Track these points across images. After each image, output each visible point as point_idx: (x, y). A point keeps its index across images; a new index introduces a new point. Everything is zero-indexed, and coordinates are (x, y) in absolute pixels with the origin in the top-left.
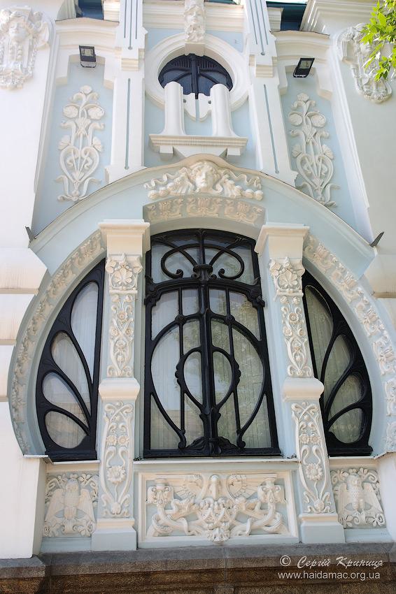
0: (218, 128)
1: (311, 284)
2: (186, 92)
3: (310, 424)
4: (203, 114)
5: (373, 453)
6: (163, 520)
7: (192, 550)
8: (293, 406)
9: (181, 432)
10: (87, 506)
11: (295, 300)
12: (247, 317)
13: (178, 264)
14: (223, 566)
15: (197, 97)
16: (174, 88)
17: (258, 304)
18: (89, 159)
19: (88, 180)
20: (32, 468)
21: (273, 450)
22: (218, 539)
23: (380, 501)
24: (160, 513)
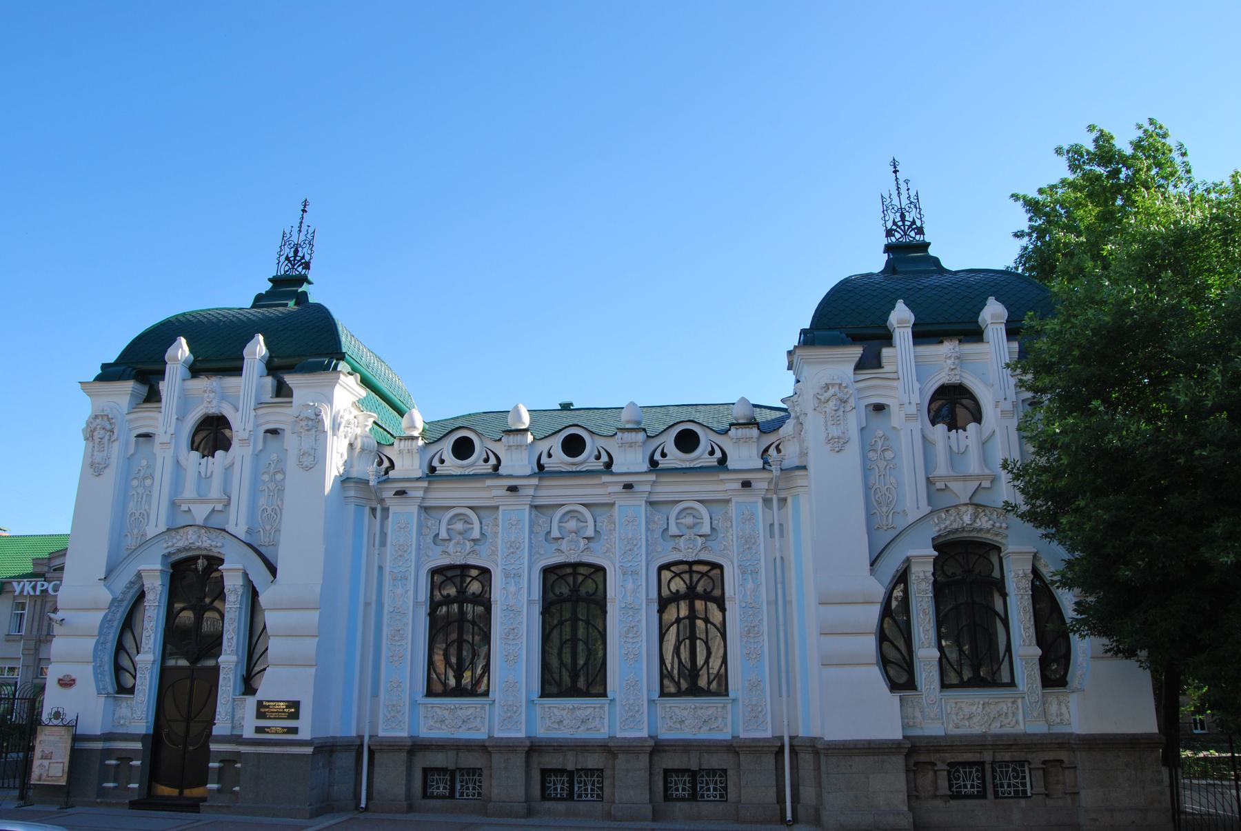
0: (973, 465)
2: (950, 430)
3: (1033, 673)
5: (1067, 687)
6: (956, 721)
7: (972, 736)
8: (1024, 663)
10: (918, 714)
11: (1026, 597)
14: (987, 743)
15: (957, 432)
16: (941, 428)
18: (890, 496)
19: (891, 513)
20: (895, 699)
21: (1012, 684)
22: (984, 731)
23: (1069, 712)
24: (954, 717)
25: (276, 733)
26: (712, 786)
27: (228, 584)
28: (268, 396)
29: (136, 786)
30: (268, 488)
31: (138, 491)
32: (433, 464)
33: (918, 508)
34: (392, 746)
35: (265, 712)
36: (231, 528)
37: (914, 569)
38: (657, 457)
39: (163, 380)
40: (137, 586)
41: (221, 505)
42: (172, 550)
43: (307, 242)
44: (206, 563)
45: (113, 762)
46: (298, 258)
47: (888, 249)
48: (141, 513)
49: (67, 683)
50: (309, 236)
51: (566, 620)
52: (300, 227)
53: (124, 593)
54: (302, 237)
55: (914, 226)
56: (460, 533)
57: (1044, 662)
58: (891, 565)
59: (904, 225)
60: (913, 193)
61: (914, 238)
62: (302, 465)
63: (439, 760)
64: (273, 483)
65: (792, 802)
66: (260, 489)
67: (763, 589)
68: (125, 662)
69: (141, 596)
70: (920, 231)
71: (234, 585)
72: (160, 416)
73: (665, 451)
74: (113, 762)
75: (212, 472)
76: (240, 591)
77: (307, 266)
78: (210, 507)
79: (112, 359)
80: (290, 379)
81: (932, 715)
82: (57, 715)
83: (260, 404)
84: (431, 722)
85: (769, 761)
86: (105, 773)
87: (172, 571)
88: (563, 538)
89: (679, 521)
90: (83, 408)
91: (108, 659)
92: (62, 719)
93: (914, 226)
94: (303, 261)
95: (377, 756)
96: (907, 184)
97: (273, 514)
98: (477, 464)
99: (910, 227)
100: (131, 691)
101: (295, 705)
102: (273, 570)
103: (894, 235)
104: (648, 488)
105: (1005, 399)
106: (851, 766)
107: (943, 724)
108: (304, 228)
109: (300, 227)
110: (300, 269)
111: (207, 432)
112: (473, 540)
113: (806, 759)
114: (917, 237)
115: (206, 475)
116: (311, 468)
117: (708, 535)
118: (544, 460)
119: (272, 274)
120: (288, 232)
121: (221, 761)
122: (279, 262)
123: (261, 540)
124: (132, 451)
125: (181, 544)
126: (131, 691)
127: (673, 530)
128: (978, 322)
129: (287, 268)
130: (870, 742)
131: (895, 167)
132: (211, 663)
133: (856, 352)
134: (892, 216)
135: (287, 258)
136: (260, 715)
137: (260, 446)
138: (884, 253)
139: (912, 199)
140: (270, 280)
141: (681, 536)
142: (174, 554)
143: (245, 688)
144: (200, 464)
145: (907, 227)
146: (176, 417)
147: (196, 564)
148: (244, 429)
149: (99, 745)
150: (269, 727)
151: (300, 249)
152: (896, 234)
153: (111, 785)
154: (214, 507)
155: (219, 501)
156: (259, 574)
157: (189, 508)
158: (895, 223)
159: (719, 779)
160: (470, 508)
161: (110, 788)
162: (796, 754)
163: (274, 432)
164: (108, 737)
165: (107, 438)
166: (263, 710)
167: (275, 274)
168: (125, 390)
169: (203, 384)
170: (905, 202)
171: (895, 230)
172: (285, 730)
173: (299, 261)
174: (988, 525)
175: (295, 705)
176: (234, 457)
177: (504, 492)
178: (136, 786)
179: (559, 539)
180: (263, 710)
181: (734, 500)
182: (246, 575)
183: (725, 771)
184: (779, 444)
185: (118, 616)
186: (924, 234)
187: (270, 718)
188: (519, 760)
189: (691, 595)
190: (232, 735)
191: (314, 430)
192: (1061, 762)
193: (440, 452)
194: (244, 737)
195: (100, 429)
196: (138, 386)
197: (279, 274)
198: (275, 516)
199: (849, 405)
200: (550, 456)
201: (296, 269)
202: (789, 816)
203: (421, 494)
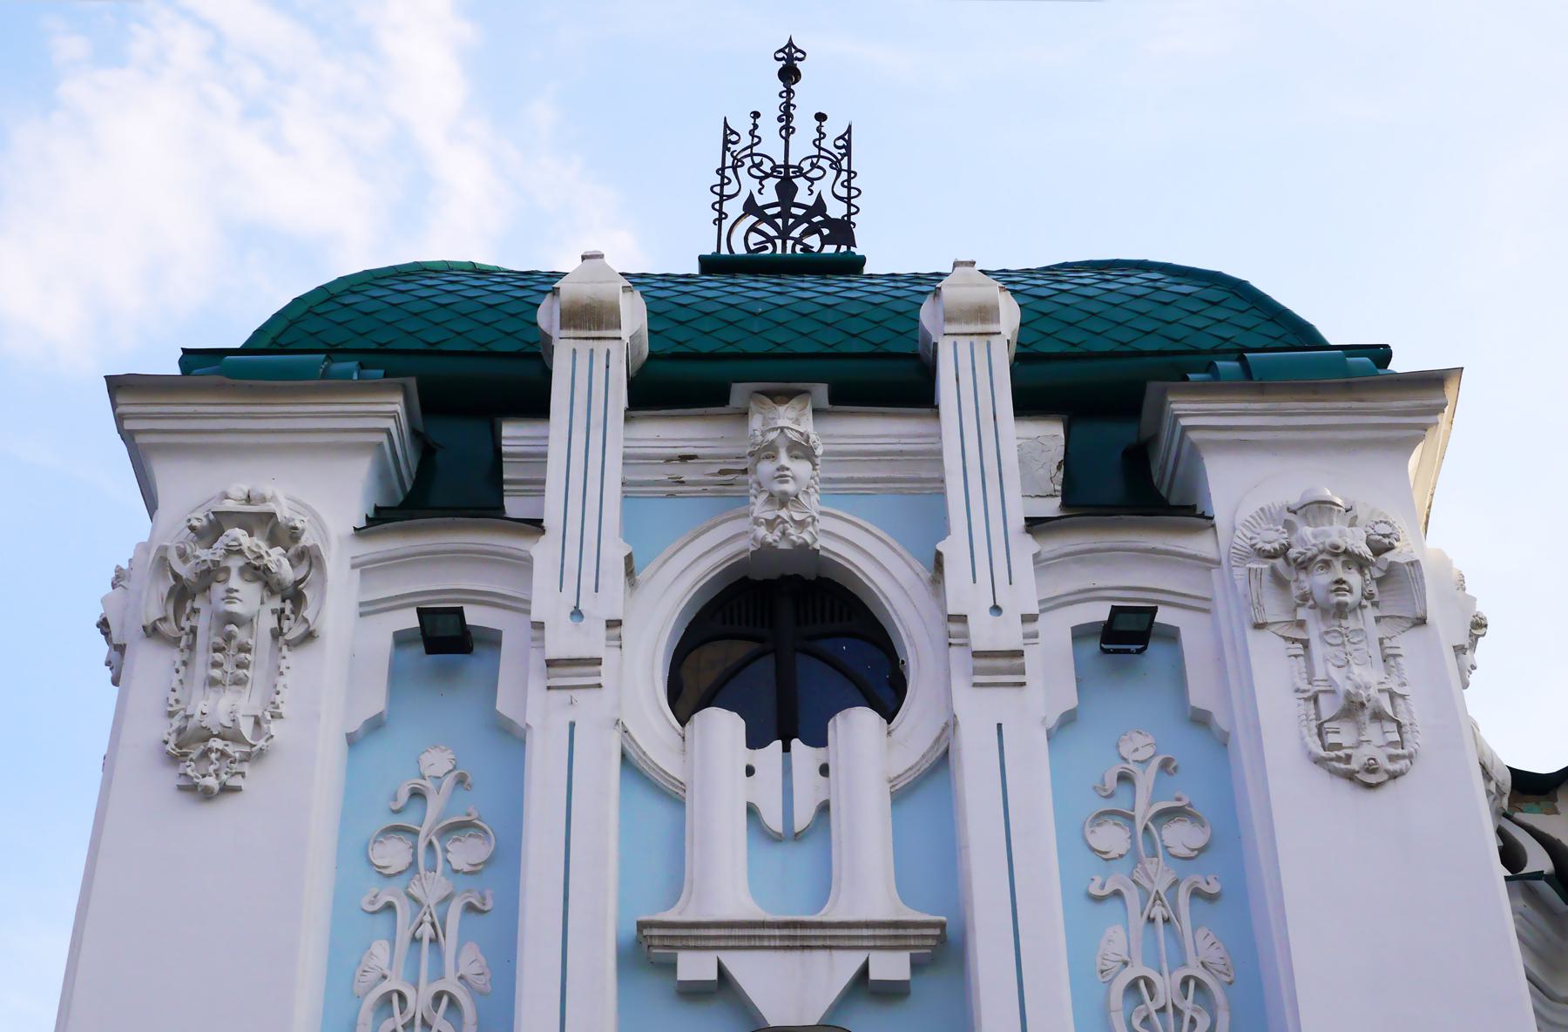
31: (415, 890)
43: (824, 163)
48: (438, 997)
50: (827, 144)
52: (786, 115)
54: (801, 148)
62: (1348, 758)
66: (1095, 890)
72: (542, 552)
75: (824, 808)
77: (842, 231)
78: (846, 965)
97: (1188, 1006)
108: (803, 121)
109: (786, 115)
111: (741, 649)
116: (1394, 776)
120: (742, 125)
122: (722, 216)
124: (376, 702)
129: (755, 238)
135: (750, 207)
144: (750, 771)
148: (996, 609)
151: (800, 182)
154: (864, 970)
155: (891, 934)
157: (721, 970)
165: (268, 622)
191: (1370, 613)
195: (242, 571)
197: (725, 251)
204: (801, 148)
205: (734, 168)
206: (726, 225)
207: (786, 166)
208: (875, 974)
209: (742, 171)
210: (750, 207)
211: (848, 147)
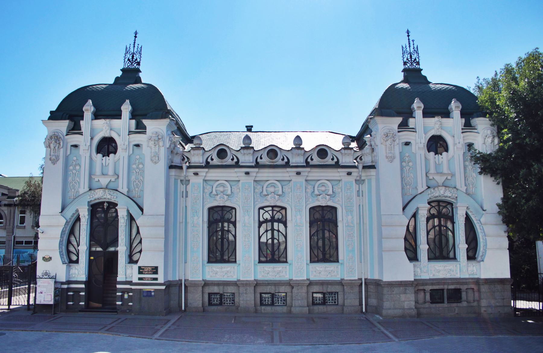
1: (468, 220)
2: (435, 155)
4: (440, 162)
9: (435, 254)
12: (449, 225)
13: (433, 211)
16: (432, 154)
17: (453, 223)
25: (148, 280)
26: (331, 299)
27: (120, 214)
28: (133, 129)
29: (83, 303)
30: (136, 171)
32: (208, 160)
33: (422, 187)
34: (195, 284)
35: (142, 271)
36: (120, 189)
37: (420, 212)
38: (309, 160)
39: (83, 119)
40: (75, 215)
41: (114, 179)
42: (92, 199)
43: (138, 52)
44: (107, 205)
45: (72, 293)
46: (134, 60)
47: (404, 71)
49: (47, 259)
50: (139, 49)
51: (269, 230)
52: (134, 45)
53: (70, 219)
54: (136, 50)
55: (415, 61)
56: (222, 192)
57: (468, 250)
58: (411, 210)
59: (411, 60)
60: (415, 47)
61: (415, 66)
63: (216, 289)
64: (138, 169)
65: (365, 305)
67: (355, 218)
68: (72, 249)
69: (78, 219)
70: (418, 63)
71: (123, 215)
73: (313, 157)
74: (72, 293)
75: (109, 163)
76: (126, 218)
77: (139, 64)
79: (54, 109)
80: (146, 122)
81: (425, 271)
82: (46, 274)
83: (130, 133)
84: (211, 274)
85: (357, 289)
86: (68, 298)
87: (91, 208)
88: (268, 195)
89: (318, 188)
90: (44, 132)
91: (64, 248)
92: (49, 276)
93: (415, 61)
94: (136, 61)
95: (189, 288)
96: (413, 42)
98: (228, 161)
99: (414, 61)
100: (77, 262)
101: (156, 268)
102: (142, 210)
103: (407, 65)
104: (306, 174)
105: (459, 143)
106: (393, 291)
107: (429, 274)
109: (134, 45)
110: (135, 65)
112: (228, 195)
113: (372, 288)
114: (417, 66)
115: (105, 165)
117: (331, 195)
118: (259, 160)
119: (122, 67)
120: (128, 47)
121: (122, 292)
122: (125, 61)
123: (134, 194)
125: (97, 197)
126: (77, 262)
127: (316, 192)
128: (448, 109)
129: (129, 65)
130: (401, 282)
131: (408, 34)
132: (112, 249)
133: (399, 120)
134: (406, 56)
135: (129, 60)
136: (140, 273)
137: (131, 152)
138: (402, 72)
139: (415, 49)
140: (121, 70)
141: (320, 195)
142: (93, 201)
143: (130, 260)
145: (412, 61)
146: (90, 138)
147: (103, 205)
149: (65, 286)
150: (144, 278)
151: (135, 55)
152: (408, 64)
153: (71, 303)
154: (111, 180)
156: (135, 211)
158: (407, 59)
159: (334, 296)
160: (226, 181)
161: (70, 305)
162: (367, 285)
163: (138, 146)
164: (69, 282)
166: (141, 270)
167: (123, 67)
168: (63, 125)
169: (101, 123)
170: (412, 50)
171: (408, 62)
172: (152, 279)
173: (134, 61)
174: (450, 195)
175: (156, 268)
176: (120, 156)
177: (244, 174)
178: (83, 303)
179: (267, 195)
180: (141, 270)
181: (343, 179)
182: (128, 211)
183: (338, 292)
184: (361, 157)
185: (68, 228)
186: (419, 65)
187: (144, 274)
188: (251, 290)
189: (323, 220)
190: (126, 281)
192: (473, 289)
193: (210, 156)
194: (133, 282)
196: (71, 122)
197: (125, 67)
198: (140, 184)
199: (396, 142)
200: (261, 158)
201: (133, 65)
202: (364, 310)
203: (204, 174)
204: (136, 50)
205: (127, 53)
206: (125, 62)
207: (133, 53)
208: (112, 180)
209: (128, 54)
210: (129, 60)
211: (141, 50)
